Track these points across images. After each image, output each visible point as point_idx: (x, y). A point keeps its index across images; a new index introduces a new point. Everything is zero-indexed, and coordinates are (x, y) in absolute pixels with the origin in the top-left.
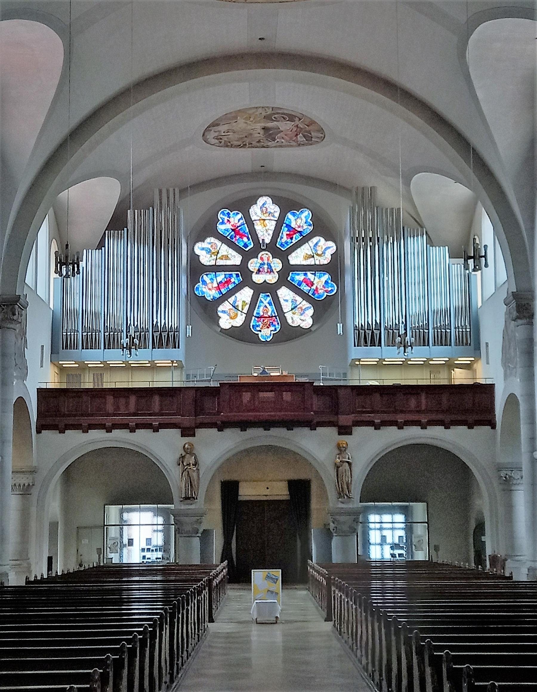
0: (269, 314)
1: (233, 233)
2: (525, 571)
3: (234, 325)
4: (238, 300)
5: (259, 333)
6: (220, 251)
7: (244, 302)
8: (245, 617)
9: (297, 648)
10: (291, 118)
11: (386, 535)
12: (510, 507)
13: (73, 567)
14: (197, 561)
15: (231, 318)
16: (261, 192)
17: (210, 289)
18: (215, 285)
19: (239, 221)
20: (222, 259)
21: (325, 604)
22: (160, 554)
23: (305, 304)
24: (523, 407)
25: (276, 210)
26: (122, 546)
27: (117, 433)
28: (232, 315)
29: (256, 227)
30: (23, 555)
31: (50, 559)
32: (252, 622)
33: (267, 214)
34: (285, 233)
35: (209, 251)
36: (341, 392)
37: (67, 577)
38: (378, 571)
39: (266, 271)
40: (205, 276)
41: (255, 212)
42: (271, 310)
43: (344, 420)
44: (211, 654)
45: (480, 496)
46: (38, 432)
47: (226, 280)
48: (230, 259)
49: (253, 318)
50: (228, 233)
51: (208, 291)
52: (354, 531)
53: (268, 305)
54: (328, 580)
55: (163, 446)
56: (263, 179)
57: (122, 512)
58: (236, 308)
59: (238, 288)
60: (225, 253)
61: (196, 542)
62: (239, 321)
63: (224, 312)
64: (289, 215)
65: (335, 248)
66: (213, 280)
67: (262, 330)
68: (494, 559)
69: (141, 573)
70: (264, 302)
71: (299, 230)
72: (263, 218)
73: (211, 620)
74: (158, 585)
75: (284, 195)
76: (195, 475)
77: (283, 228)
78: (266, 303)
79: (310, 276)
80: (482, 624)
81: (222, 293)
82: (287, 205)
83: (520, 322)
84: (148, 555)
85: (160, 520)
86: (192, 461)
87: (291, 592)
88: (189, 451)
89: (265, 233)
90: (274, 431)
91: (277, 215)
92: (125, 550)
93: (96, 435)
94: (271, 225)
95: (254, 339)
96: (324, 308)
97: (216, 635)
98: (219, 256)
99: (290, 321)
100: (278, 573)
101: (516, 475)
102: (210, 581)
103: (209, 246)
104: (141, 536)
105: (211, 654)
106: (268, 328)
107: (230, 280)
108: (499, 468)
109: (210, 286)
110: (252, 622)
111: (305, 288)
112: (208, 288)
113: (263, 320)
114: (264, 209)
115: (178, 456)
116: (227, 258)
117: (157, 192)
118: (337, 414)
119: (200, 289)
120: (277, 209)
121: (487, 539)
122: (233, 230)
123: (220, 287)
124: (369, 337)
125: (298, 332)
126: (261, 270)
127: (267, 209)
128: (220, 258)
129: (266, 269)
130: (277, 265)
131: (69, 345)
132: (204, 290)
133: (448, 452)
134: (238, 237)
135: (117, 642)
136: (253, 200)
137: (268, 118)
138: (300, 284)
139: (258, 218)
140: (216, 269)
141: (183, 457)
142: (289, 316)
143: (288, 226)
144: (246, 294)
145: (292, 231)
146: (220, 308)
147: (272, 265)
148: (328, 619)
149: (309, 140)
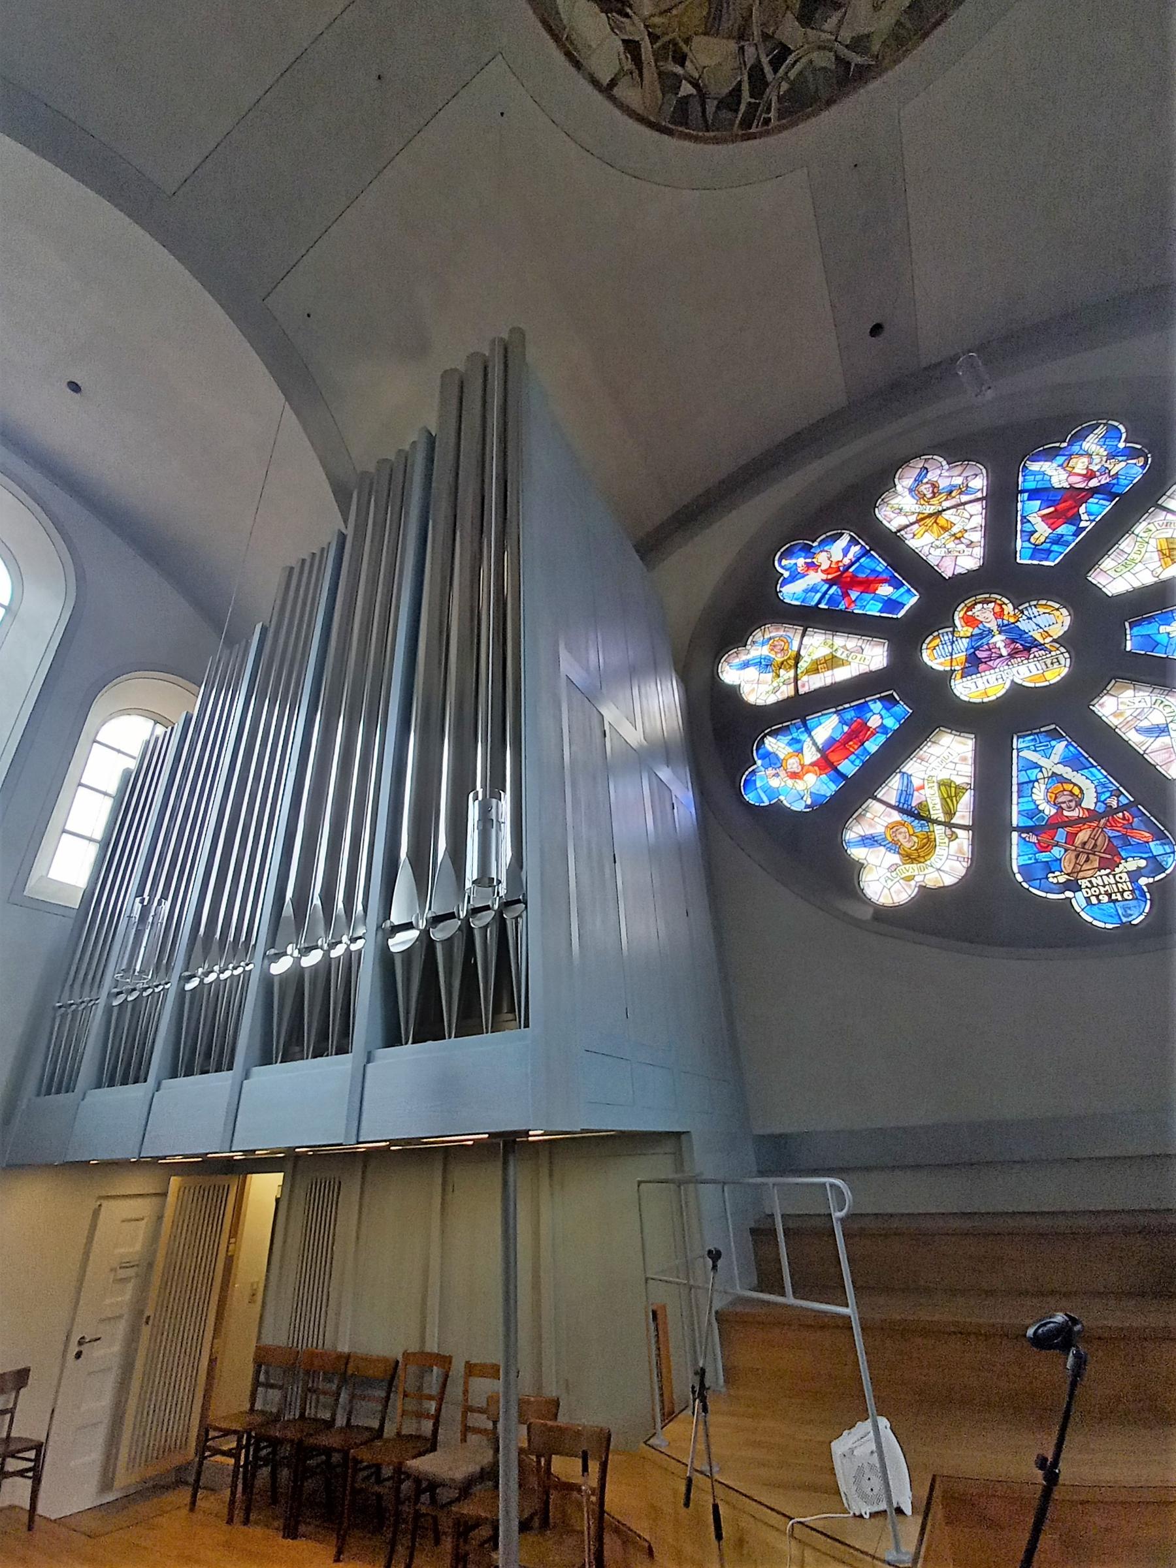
0: (1089, 802)
1: (834, 588)
3: (930, 884)
4: (916, 782)
5: (1069, 894)
6: (802, 653)
7: (945, 784)
15: (910, 858)
17: (794, 776)
18: (810, 755)
19: (846, 552)
20: (817, 671)
28: (907, 845)
33: (943, 496)
34: (1036, 519)
35: (765, 665)
39: (1004, 652)
40: (771, 743)
42: (1090, 787)
47: (846, 729)
48: (841, 663)
49: (1015, 835)
50: (819, 595)
51: (790, 782)
53: (1067, 772)
58: (918, 814)
60: (824, 651)
62: (949, 864)
63: (869, 841)
66: (798, 741)
67: (1084, 883)
70: (1043, 762)
71: (1094, 483)
72: (930, 509)
77: (1020, 505)
81: (843, 776)
95: (1060, 930)
98: (803, 665)
103: (765, 651)
106: (1110, 863)
107: (864, 727)
109: (793, 765)
112: (789, 776)
113: (1071, 837)
114: (925, 489)
116: (832, 662)
119: (758, 784)
122: (831, 583)
123: (833, 758)
126: (980, 654)
127: (934, 485)
128: (808, 672)
129: (1000, 645)
132: (774, 783)
134: (854, 595)
139: (913, 518)
146: (853, 833)
147: (1023, 625)
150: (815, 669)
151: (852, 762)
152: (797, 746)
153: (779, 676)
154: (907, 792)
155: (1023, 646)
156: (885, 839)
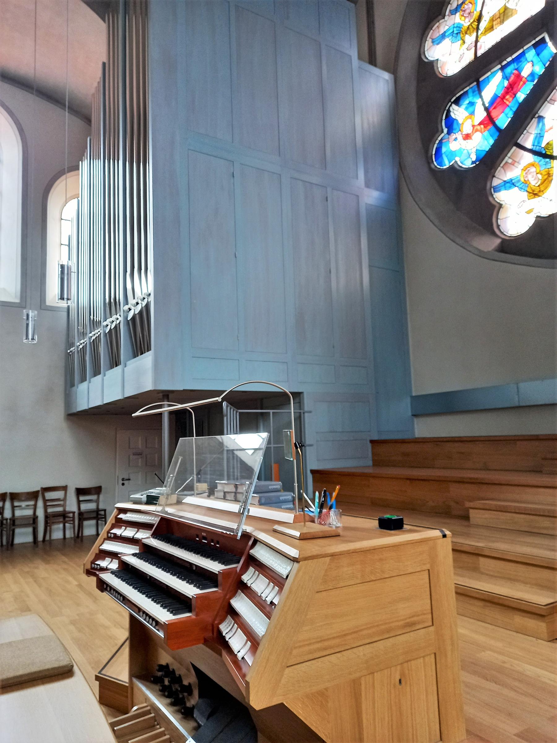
15: (534, 194)
17: (467, 137)
81: (498, 129)
98: (483, 25)
107: (518, 77)
123: (494, 114)
150: (490, 28)
151: (506, 115)
152: (471, 109)
153: (464, 42)
154: (540, 137)
156: (519, 181)
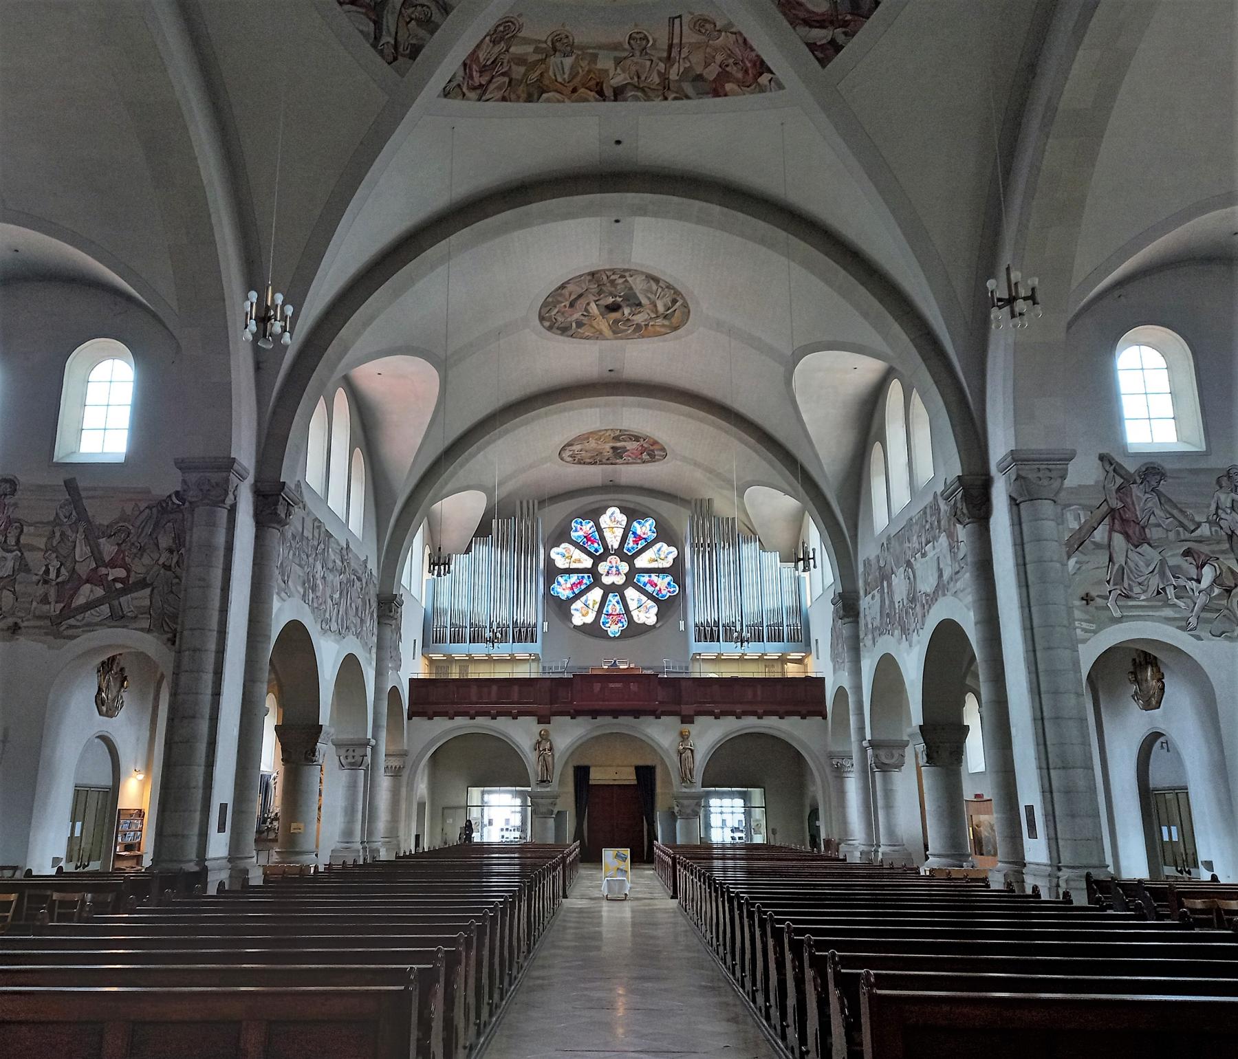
2: (858, 854)
8: (596, 894)
9: (644, 922)
10: (637, 439)
11: (727, 819)
12: (842, 793)
13: (438, 844)
14: (551, 841)
16: (611, 503)
21: (670, 883)
22: (517, 834)
23: (650, 603)
24: (851, 700)
25: (623, 519)
26: (483, 826)
27: (480, 720)
29: (606, 534)
30: (393, 833)
31: (417, 837)
32: (602, 898)
36: (683, 683)
37: (433, 853)
38: (720, 851)
40: (560, 579)
41: (604, 520)
42: (619, 608)
43: (687, 709)
44: (565, 928)
45: (814, 782)
46: (409, 718)
52: (697, 814)
54: (674, 859)
55: (521, 733)
56: (612, 490)
57: (483, 793)
59: (589, 588)
61: (551, 822)
62: (590, 619)
64: (635, 524)
65: (676, 552)
68: (828, 843)
69: (500, 851)
73: (565, 896)
74: (517, 861)
75: (632, 506)
76: (550, 759)
78: (614, 602)
79: (654, 577)
80: (819, 900)
82: (633, 514)
83: (847, 620)
84: (506, 834)
85: (518, 801)
86: (548, 746)
87: (639, 872)
88: (544, 737)
89: (613, 540)
90: (622, 720)
91: (624, 523)
92: (485, 829)
93: (460, 721)
94: (619, 533)
95: (604, 635)
96: (667, 607)
97: (570, 910)
99: (636, 619)
100: (627, 852)
101: (847, 763)
102: (564, 859)
104: (500, 816)
105: (565, 928)
108: (831, 756)
110: (602, 898)
111: (649, 588)
112: (563, 588)
115: (534, 741)
116: (579, 561)
117: (518, 503)
118: (679, 704)
120: (625, 518)
121: (821, 824)
124: (708, 633)
125: (644, 629)
130: (624, 567)
131: (440, 640)
133: (789, 746)
135: (480, 910)
136: (602, 510)
137: (616, 439)
138: (645, 585)
140: (569, 571)
141: (539, 743)
142: (635, 614)
143: (634, 533)
144: (597, 594)
145: (638, 538)
146: (573, 607)
148: (674, 896)
149: (653, 458)
155: (618, 573)
